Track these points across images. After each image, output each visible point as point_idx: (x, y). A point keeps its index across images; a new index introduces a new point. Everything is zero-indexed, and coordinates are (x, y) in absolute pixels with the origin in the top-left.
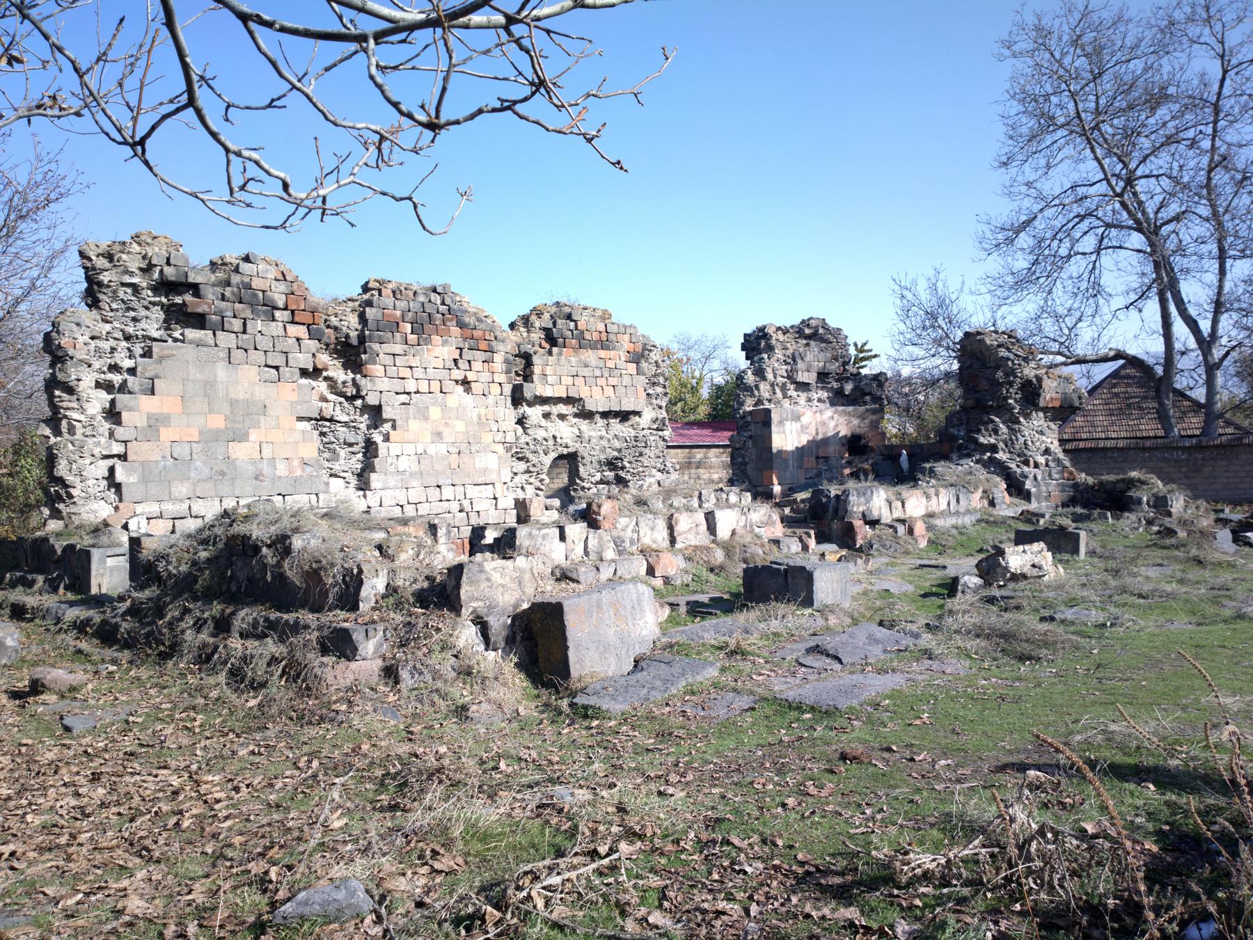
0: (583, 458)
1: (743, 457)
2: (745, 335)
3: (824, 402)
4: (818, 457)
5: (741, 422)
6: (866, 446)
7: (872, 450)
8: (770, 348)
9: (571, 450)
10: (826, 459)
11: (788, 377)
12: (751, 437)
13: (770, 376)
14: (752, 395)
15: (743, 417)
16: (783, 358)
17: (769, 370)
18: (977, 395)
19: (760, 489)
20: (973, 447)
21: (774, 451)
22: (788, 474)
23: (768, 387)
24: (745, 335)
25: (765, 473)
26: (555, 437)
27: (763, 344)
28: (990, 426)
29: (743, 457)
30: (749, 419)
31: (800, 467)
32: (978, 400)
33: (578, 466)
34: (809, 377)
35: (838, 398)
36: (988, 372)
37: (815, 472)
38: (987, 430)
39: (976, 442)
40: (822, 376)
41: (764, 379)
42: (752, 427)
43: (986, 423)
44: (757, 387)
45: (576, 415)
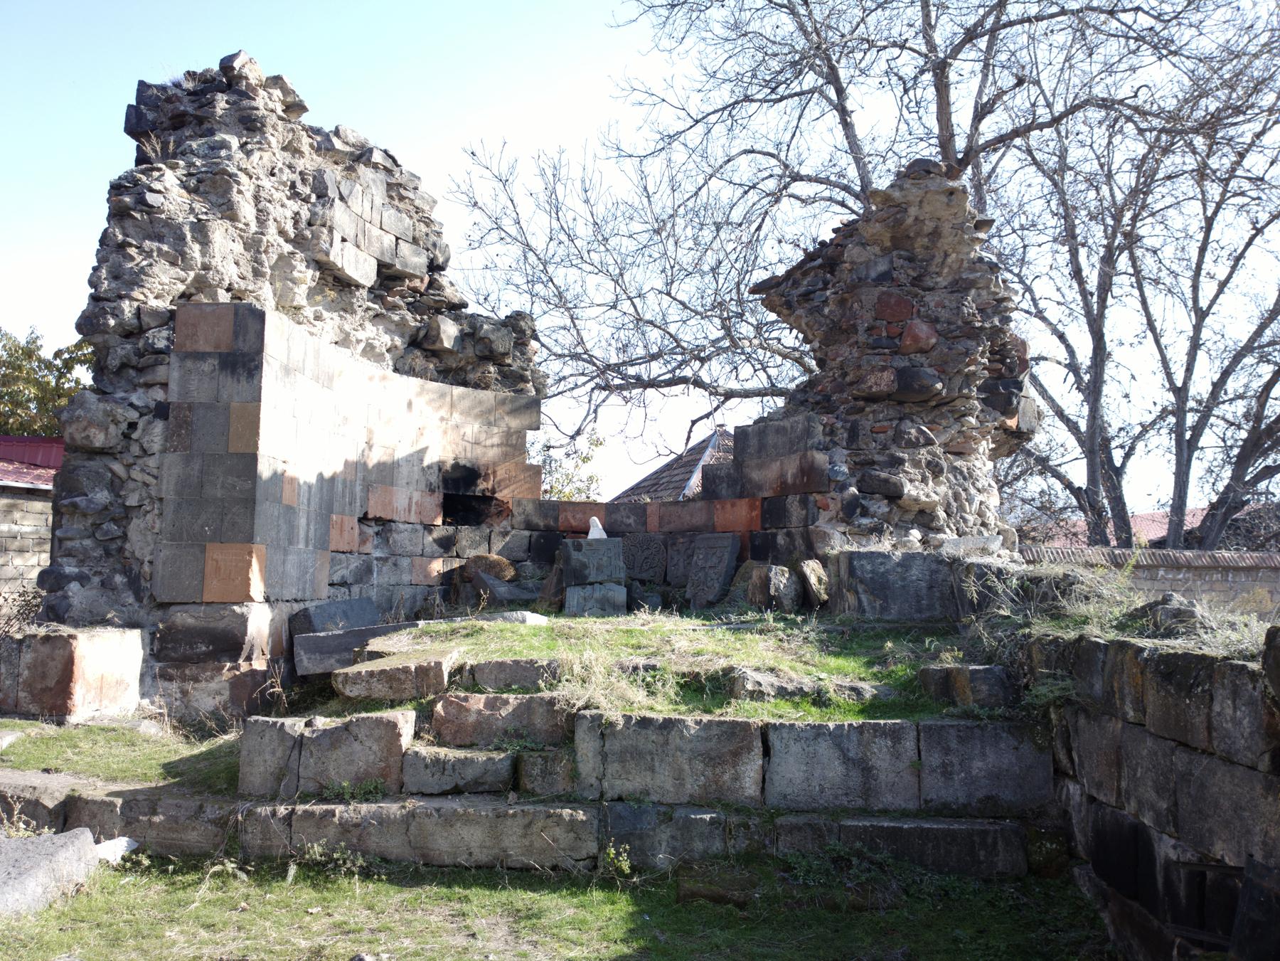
1: (116, 485)
2: (143, 86)
3: (379, 358)
4: (364, 519)
5: (123, 350)
6: (487, 499)
7: (504, 511)
8: (250, 124)
10: (384, 524)
11: (298, 241)
12: (161, 411)
13: (247, 211)
14: (179, 258)
15: (133, 332)
16: (287, 175)
17: (247, 185)
18: (902, 363)
19: (183, 618)
20: (881, 507)
21: (265, 469)
22: (292, 569)
23: (239, 247)
24: (143, 86)
25: (217, 554)
27: (221, 103)
28: (923, 454)
29: (116, 485)
30: (159, 338)
31: (322, 543)
35: (420, 353)
36: (931, 299)
37: (355, 562)
38: (916, 464)
39: (894, 495)
40: (388, 277)
41: (229, 212)
42: (171, 372)
43: (914, 445)
44: (201, 230)
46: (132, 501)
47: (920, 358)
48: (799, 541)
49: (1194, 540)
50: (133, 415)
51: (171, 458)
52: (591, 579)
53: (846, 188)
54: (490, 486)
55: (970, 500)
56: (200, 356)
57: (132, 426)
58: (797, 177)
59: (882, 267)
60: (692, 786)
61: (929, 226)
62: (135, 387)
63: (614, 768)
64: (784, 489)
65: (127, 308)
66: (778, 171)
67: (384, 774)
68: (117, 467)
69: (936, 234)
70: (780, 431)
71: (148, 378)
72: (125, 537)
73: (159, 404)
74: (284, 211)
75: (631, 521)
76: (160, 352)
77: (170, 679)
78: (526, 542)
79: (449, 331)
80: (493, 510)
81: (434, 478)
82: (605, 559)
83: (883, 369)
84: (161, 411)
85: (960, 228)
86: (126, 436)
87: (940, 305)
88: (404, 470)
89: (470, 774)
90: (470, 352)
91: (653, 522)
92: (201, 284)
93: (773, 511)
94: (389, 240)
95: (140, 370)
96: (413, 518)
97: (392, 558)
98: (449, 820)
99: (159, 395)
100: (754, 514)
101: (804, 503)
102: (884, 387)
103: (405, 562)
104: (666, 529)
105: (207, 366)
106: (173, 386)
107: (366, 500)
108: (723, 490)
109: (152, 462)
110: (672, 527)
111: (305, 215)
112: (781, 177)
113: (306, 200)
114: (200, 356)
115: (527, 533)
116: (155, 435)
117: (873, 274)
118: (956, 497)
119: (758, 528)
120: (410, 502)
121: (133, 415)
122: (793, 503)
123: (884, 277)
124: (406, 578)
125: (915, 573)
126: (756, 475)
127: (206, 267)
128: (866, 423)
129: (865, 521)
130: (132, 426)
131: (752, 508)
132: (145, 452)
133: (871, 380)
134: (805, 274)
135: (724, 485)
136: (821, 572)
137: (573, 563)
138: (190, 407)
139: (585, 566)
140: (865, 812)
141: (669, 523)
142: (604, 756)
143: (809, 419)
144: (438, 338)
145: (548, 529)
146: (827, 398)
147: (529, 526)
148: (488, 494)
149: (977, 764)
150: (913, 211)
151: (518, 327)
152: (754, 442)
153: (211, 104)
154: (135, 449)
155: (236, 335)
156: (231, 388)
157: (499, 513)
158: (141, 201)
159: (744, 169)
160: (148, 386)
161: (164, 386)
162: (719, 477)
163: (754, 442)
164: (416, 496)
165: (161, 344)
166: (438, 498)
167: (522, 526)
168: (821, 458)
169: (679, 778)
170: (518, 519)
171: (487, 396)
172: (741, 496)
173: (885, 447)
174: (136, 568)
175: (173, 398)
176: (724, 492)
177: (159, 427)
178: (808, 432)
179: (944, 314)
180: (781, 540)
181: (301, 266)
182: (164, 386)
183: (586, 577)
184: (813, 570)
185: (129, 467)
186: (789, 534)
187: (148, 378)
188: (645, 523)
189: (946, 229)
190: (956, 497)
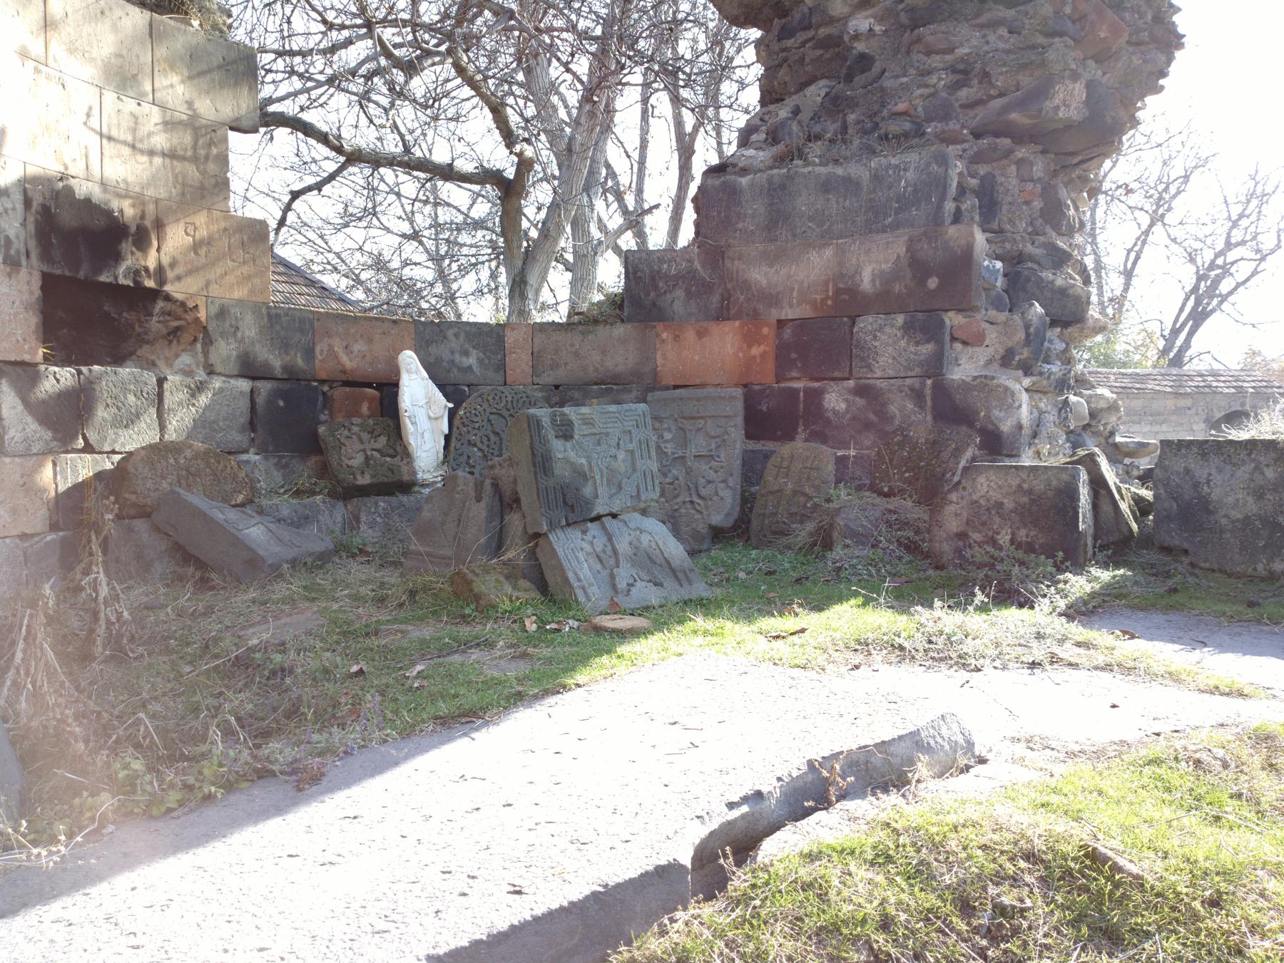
6: (142, 297)
7: (185, 329)
52: (599, 509)
54: (151, 263)
75: (472, 361)
78: (244, 404)
80: (155, 325)
82: (621, 455)
91: (519, 363)
100: (755, 351)
104: (548, 378)
108: (677, 301)
110: (560, 375)
115: (244, 385)
119: (769, 379)
128: (1009, 179)
131: (750, 339)
135: (680, 293)
137: (560, 470)
141: (555, 366)
145: (292, 376)
147: (249, 369)
148: (150, 283)
152: (755, 209)
162: (666, 277)
163: (755, 209)
167: (233, 367)
170: (225, 350)
172: (722, 315)
176: (678, 307)
180: (836, 400)
183: (588, 504)
188: (502, 367)
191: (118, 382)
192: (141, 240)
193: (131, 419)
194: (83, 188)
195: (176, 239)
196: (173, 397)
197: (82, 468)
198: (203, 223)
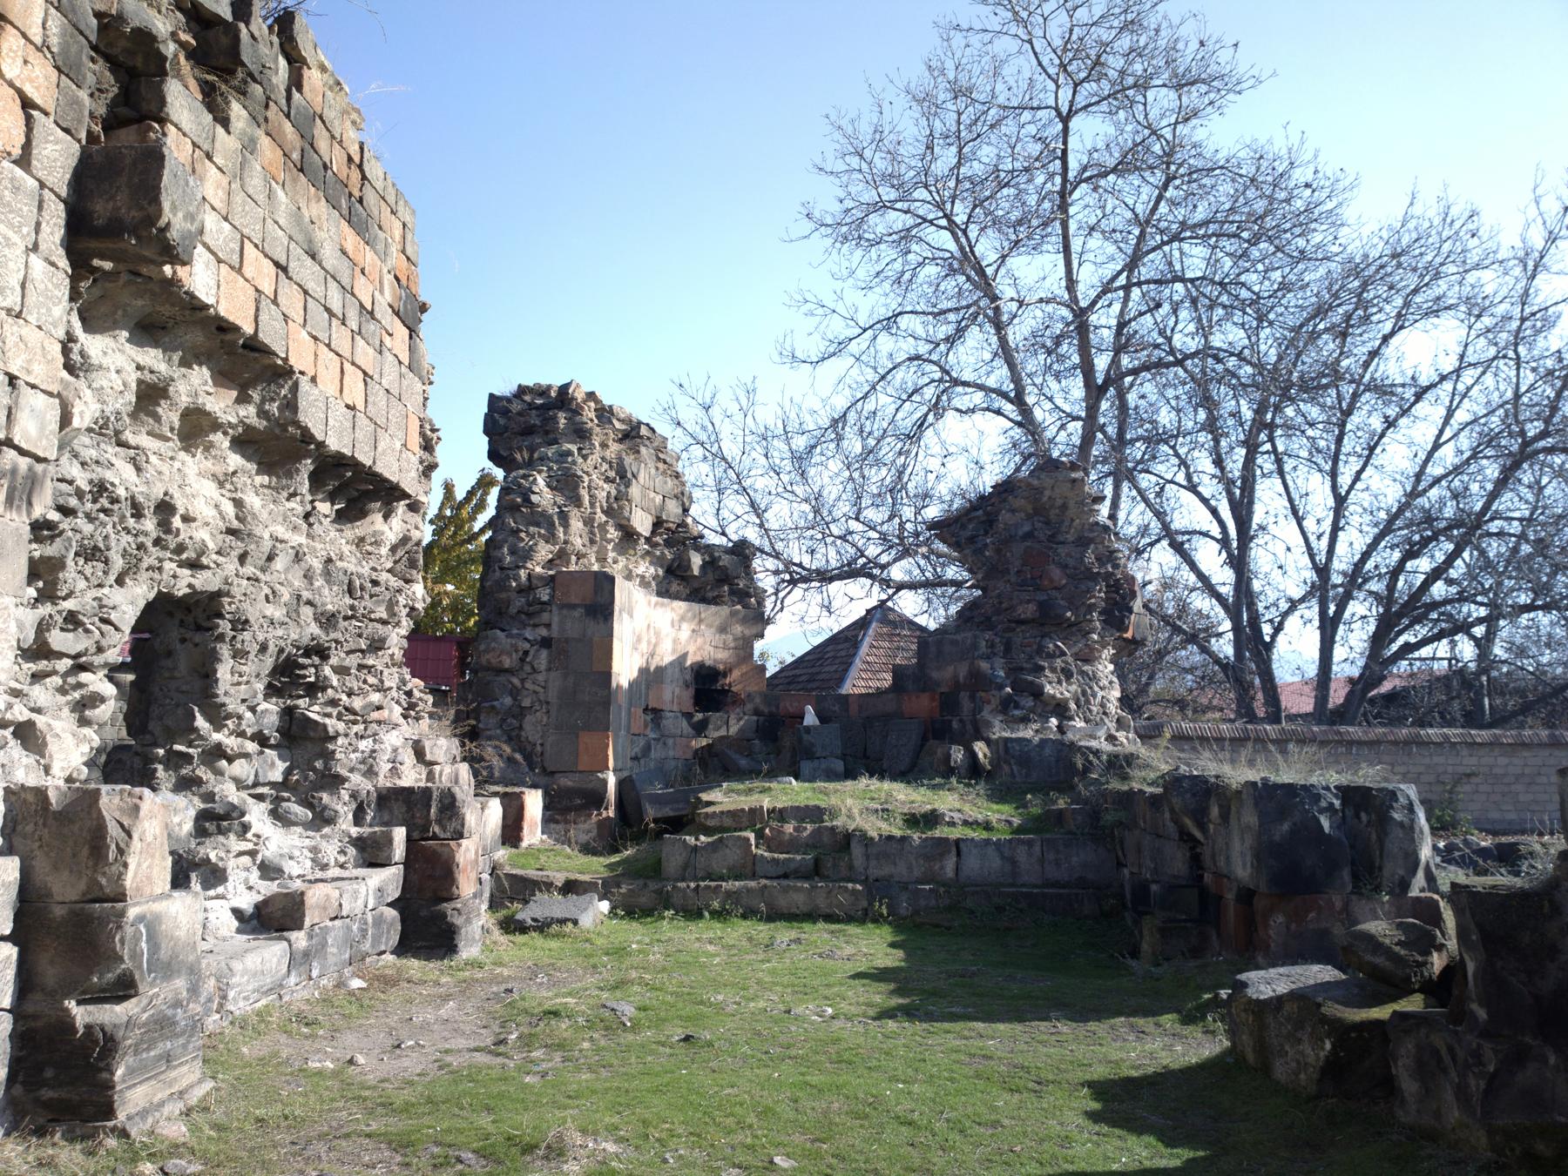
0: (241, 624)
1: (515, 693)
2: (493, 399)
4: (646, 710)
5: (519, 602)
6: (725, 692)
7: (737, 701)
9: (206, 581)
11: (608, 512)
12: (546, 643)
14: (551, 538)
18: (1042, 597)
19: (566, 782)
20: (1028, 702)
24: (492, 396)
25: (586, 739)
26: (165, 509)
28: (1059, 663)
29: (515, 693)
32: (1044, 607)
33: (215, 658)
34: (642, 523)
36: (1062, 550)
38: (1053, 670)
39: (1038, 693)
41: (578, 503)
43: (1051, 656)
44: (564, 517)
45: (245, 442)
46: (526, 703)
47: (1054, 593)
48: (969, 727)
49: (1341, 715)
50: (527, 646)
51: (553, 674)
53: (1004, 395)
55: (1094, 696)
56: (573, 607)
57: (526, 653)
58: (956, 382)
59: (1027, 528)
60: (917, 873)
61: (1059, 502)
62: (525, 626)
63: (873, 863)
64: (957, 686)
65: (523, 573)
66: (937, 375)
67: (744, 866)
68: (516, 681)
69: (1064, 507)
70: (954, 643)
71: (536, 621)
72: (521, 728)
73: (544, 639)
74: (604, 490)
76: (544, 603)
77: (557, 822)
79: (696, 561)
80: (729, 700)
81: (688, 677)
83: (1029, 602)
84: (546, 643)
85: (1082, 503)
86: (522, 660)
87: (1068, 555)
88: (669, 671)
89: (792, 866)
90: (710, 576)
91: (854, 709)
92: (562, 556)
93: (949, 703)
94: (658, 499)
95: (529, 615)
96: (675, 708)
97: (662, 738)
98: (786, 890)
99: (544, 632)
101: (972, 698)
102: (1029, 615)
103: (670, 741)
105: (577, 613)
106: (555, 626)
107: (647, 695)
109: (541, 678)
111: (614, 492)
112: (941, 381)
113: (613, 481)
114: (573, 607)
116: (542, 658)
117: (1020, 533)
118: (1084, 693)
120: (674, 696)
121: (527, 646)
122: (964, 697)
123: (1029, 535)
124: (671, 753)
125: (1047, 751)
126: (935, 675)
127: (566, 542)
128: (1017, 640)
129: (1017, 712)
130: (526, 653)
131: (933, 699)
132: (534, 670)
133: (1020, 610)
134: (970, 520)
136: (986, 750)
138: (567, 641)
139: (813, 745)
140: (1012, 885)
142: (867, 857)
143: (975, 637)
144: (689, 567)
145: (771, 715)
146: (988, 619)
147: (757, 712)
149: (1075, 859)
150: (1047, 493)
151: (742, 551)
152: (933, 649)
153: (555, 419)
154: (527, 668)
155: (596, 592)
156: (593, 627)
157: (734, 703)
158: (527, 500)
159: (906, 376)
160: (535, 626)
161: (548, 626)
163: (933, 649)
164: (677, 691)
165: (545, 598)
166: (691, 691)
168: (984, 665)
169: (910, 868)
170: (749, 707)
171: (724, 610)
172: (924, 691)
173: (1031, 657)
174: (529, 748)
175: (555, 633)
177: (544, 653)
178: (975, 646)
179: (1071, 562)
180: (955, 725)
181: (612, 530)
182: (548, 626)
184: (980, 748)
185: (523, 681)
186: (961, 721)
187: (536, 621)
189: (1071, 504)
190: (1084, 693)
191: (715, 717)
192: (725, 674)
193: (719, 728)
194: (708, 663)
195: (736, 674)
196: (732, 722)
197: (704, 742)
198: (744, 668)
